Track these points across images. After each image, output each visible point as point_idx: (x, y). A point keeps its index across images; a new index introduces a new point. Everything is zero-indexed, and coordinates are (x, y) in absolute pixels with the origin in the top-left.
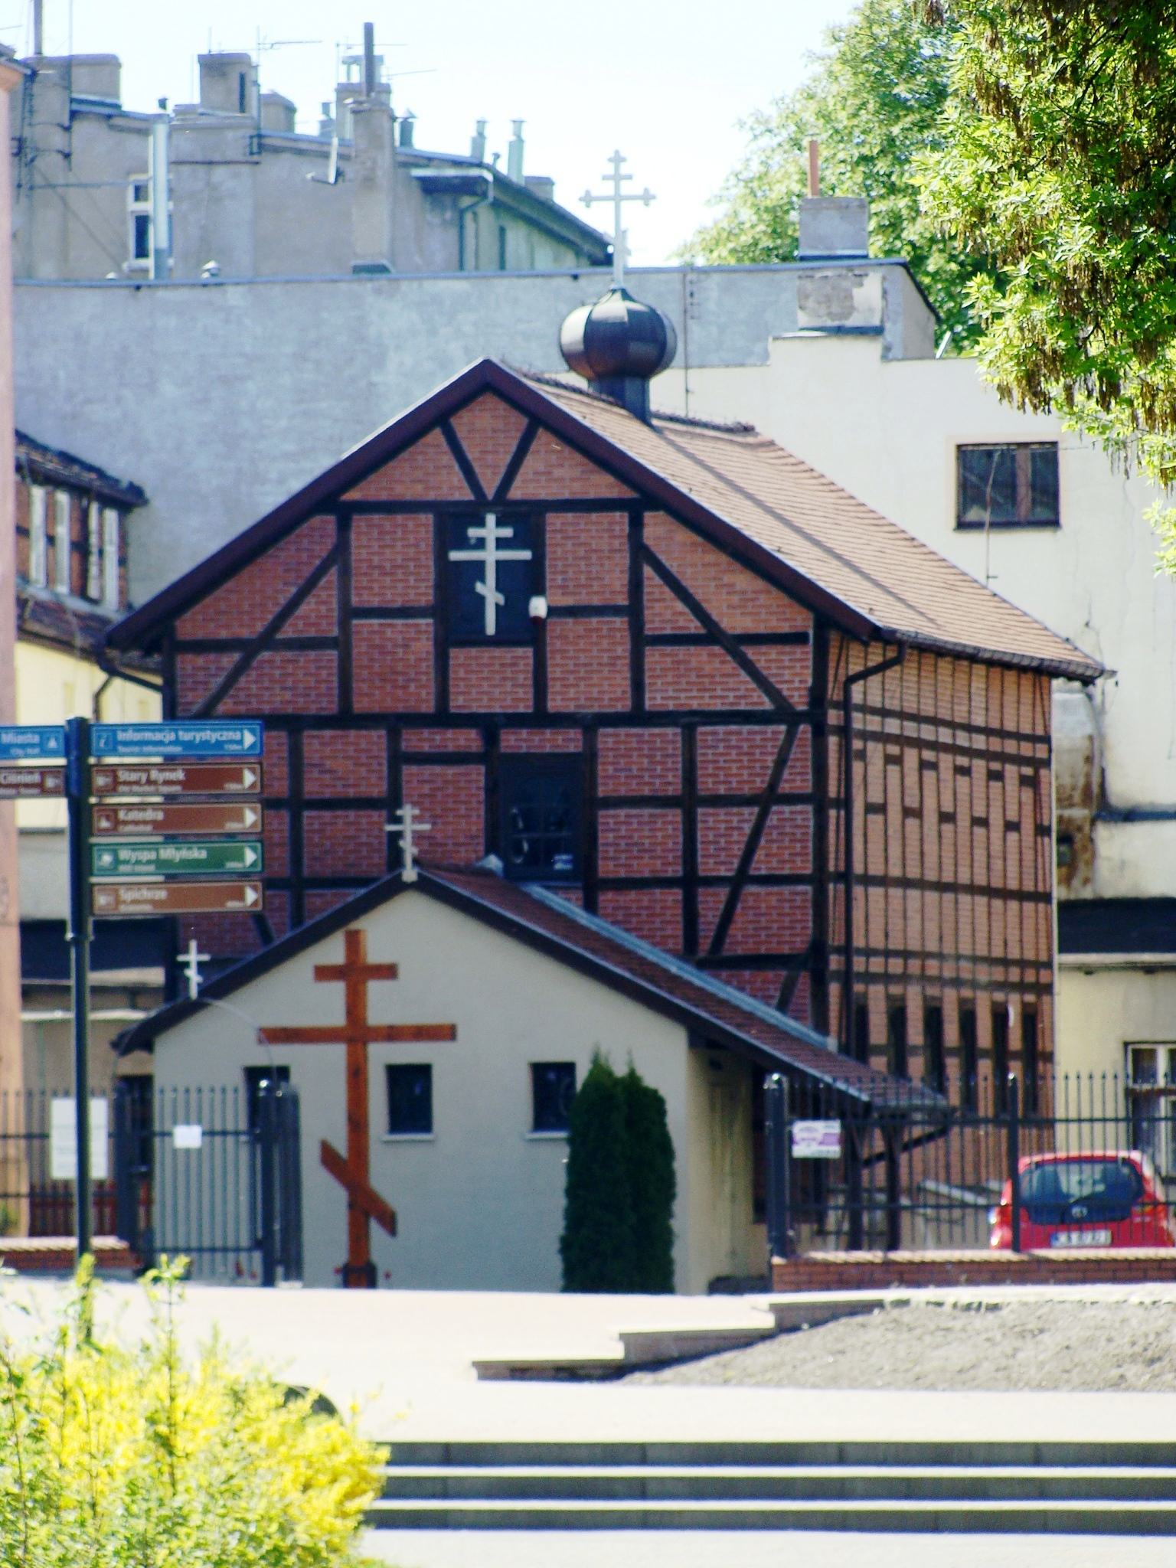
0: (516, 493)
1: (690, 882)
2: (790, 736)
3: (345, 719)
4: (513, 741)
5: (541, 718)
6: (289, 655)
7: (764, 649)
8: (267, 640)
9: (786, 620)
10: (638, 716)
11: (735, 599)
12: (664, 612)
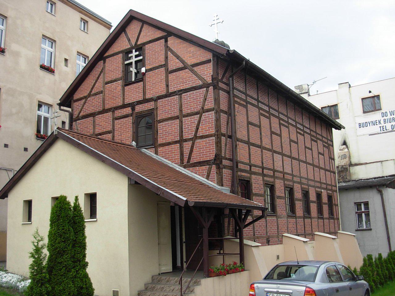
1: (181, 141)
2: (207, 91)
4: (139, 108)
8: (89, 95)
10: (168, 95)
11: (191, 55)
12: (174, 63)
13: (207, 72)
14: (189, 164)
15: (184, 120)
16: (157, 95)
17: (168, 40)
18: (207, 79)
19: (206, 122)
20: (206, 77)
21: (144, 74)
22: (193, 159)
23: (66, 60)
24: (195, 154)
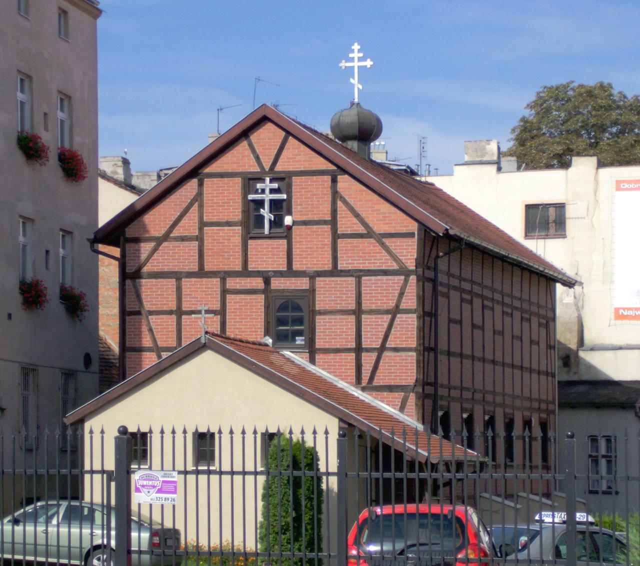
0: (279, 168)
3: (201, 273)
4: (277, 284)
5: (290, 272)
6: (177, 244)
7: (394, 240)
9: (404, 227)
10: (335, 272)
12: (347, 223)
13: (408, 252)
14: (371, 385)
15: (365, 318)
16: (316, 269)
17: (338, 180)
18: (407, 263)
19: (403, 328)
20: (405, 259)
21: (289, 228)
22: (378, 379)
23: (45, 114)
24: (382, 373)
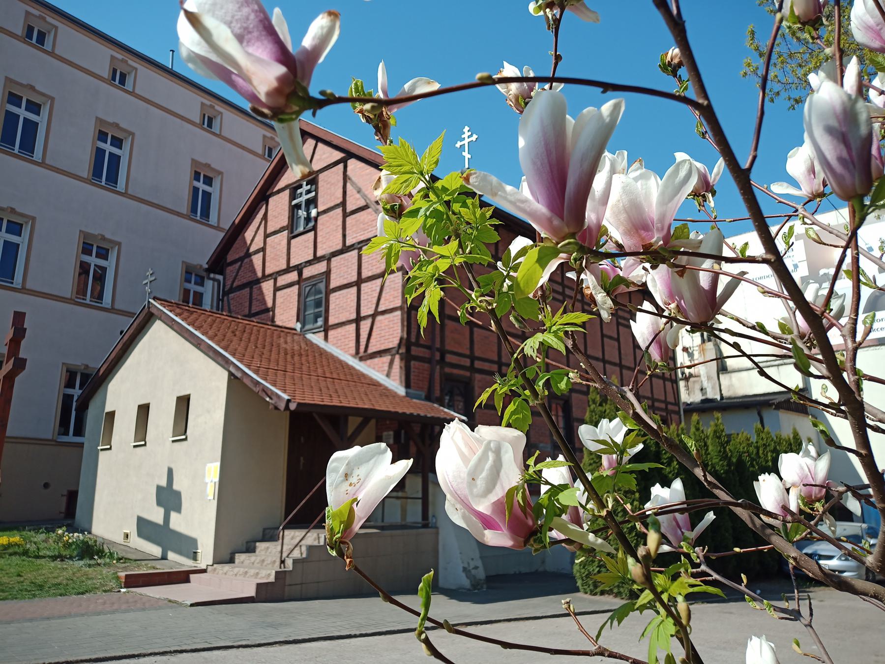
4: (307, 272)
5: (316, 259)
